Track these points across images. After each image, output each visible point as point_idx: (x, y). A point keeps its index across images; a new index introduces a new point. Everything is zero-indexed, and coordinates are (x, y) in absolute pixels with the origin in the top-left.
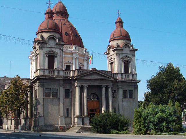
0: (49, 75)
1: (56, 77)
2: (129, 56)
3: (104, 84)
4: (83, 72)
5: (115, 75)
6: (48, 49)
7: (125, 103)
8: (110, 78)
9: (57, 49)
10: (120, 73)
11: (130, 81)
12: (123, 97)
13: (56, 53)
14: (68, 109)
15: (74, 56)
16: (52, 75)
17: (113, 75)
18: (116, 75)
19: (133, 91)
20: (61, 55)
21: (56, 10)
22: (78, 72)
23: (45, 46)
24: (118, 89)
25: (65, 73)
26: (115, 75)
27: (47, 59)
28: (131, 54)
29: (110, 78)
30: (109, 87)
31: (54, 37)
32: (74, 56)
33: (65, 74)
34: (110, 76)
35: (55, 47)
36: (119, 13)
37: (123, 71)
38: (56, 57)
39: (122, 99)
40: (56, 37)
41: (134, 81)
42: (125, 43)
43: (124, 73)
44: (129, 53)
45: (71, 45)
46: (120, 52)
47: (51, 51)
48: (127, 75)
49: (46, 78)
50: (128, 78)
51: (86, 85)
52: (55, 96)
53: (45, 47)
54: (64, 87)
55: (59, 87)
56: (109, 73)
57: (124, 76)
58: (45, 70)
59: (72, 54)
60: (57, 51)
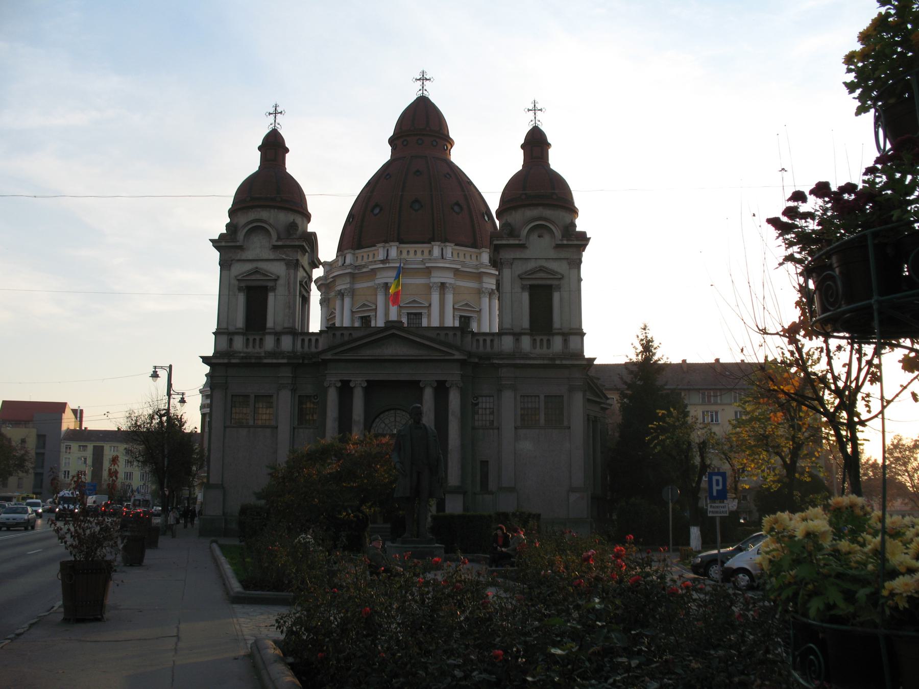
0: (245, 350)
1: (265, 358)
2: (554, 266)
5: (492, 341)
6: (248, 267)
7: (526, 446)
8: (454, 355)
10: (510, 334)
11: (546, 362)
13: (274, 277)
15: (437, 278)
16: (257, 349)
17: (485, 340)
18: (496, 342)
20: (289, 283)
22: (334, 335)
23: (238, 257)
25: (303, 340)
26: (492, 341)
27: (241, 298)
28: (560, 259)
29: (454, 355)
30: (447, 385)
33: (302, 347)
34: (450, 346)
35: (272, 257)
36: (535, 110)
37: (526, 324)
38: (274, 289)
39: (516, 428)
40: (270, 225)
41: (564, 362)
43: (529, 331)
44: (552, 254)
46: (518, 254)
48: (542, 340)
49: (233, 361)
51: (358, 380)
54: (294, 391)
56: (451, 333)
57: (526, 343)
60: (278, 269)
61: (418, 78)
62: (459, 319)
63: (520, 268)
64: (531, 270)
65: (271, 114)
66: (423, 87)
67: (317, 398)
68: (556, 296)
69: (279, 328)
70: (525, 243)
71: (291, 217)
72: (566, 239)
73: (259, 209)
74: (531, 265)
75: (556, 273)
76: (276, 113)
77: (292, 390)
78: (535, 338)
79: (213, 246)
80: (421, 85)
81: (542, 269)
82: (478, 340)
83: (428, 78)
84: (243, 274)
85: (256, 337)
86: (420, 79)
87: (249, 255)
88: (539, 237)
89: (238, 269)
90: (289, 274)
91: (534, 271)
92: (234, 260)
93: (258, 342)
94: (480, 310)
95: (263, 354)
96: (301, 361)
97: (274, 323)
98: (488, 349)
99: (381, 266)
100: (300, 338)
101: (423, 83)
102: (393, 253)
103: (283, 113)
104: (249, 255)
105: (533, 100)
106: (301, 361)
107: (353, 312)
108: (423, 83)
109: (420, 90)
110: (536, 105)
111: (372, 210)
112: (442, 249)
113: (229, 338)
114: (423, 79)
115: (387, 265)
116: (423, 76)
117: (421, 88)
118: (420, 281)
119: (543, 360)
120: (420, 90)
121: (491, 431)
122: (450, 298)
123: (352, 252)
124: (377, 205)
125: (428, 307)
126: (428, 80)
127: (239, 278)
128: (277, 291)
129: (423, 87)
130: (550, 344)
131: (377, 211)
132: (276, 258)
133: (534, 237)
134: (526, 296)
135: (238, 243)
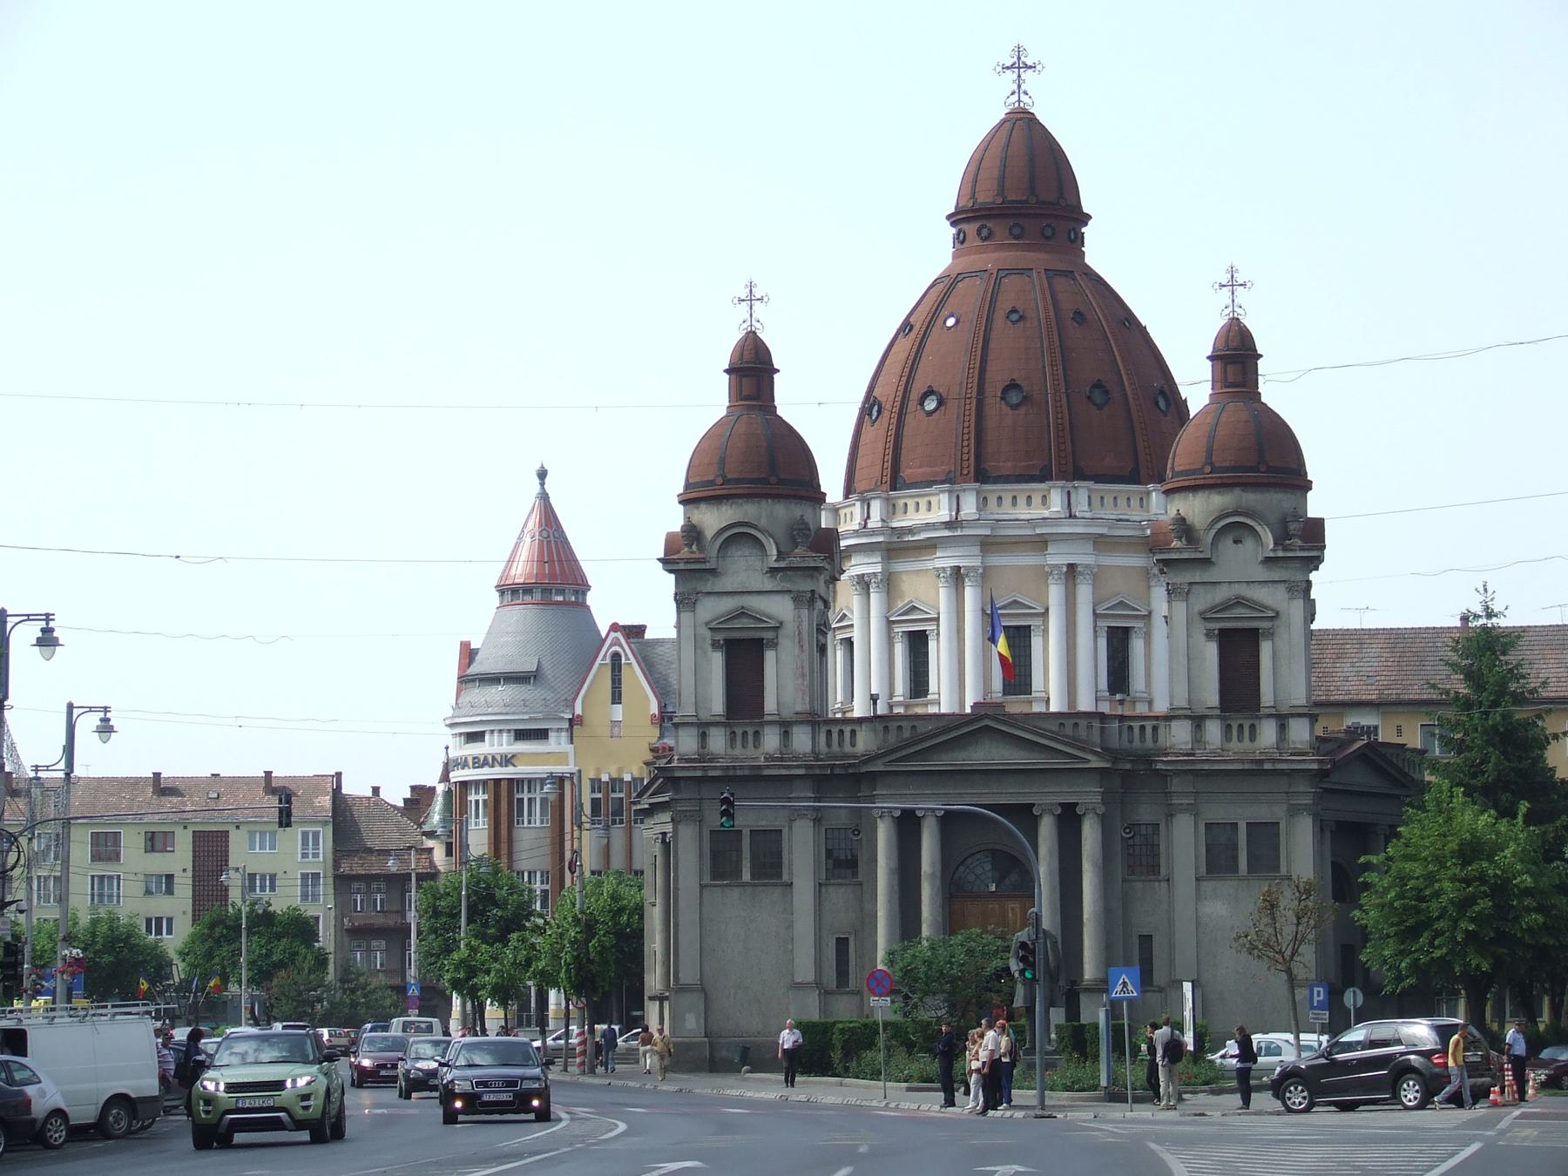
2: (1262, 595)
3: (1047, 797)
4: (914, 727)
5: (1155, 729)
6: (728, 604)
8: (1089, 761)
9: (778, 598)
10: (1186, 717)
11: (1247, 766)
12: (1203, 870)
13: (773, 624)
14: (842, 944)
16: (751, 751)
18: (1161, 731)
19: (1282, 826)
20: (800, 633)
21: (973, 196)
22: (886, 728)
23: (708, 588)
24: (1170, 816)
25: (829, 733)
26: (1155, 729)
27: (717, 661)
29: (1089, 761)
30: (1079, 811)
31: (753, 532)
32: (1058, 557)
33: (829, 744)
38: (774, 644)
39: (1197, 879)
42: (1235, 513)
43: (1217, 712)
44: (1262, 573)
45: (1043, 477)
47: (742, 613)
48: (1241, 726)
50: (1247, 742)
52: (770, 866)
53: (709, 593)
55: (791, 821)
57: (1213, 731)
58: (709, 724)
59: (1041, 543)
60: (780, 608)
61: (1009, 64)
62: (1105, 634)
63: (1204, 599)
64: (1222, 604)
65: (743, 300)
66: (1019, 86)
67: (858, 834)
68: (1266, 648)
69: (787, 714)
70: (1209, 556)
71: (799, 510)
72: (1280, 548)
73: (740, 501)
74: (1221, 594)
75: (1262, 607)
76: (751, 299)
77: (814, 820)
78: (1229, 722)
79: (666, 570)
80: (1014, 82)
81: (1239, 602)
82: (1131, 728)
83: (1029, 63)
84: (717, 619)
85: (747, 729)
86: (1012, 67)
87: (727, 583)
88: (1235, 542)
89: (711, 609)
90: (799, 617)
91: (1227, 606)
92: (701, 592)
93: (750, 738)
94: (1150, 613)
95: (762, 762)
96: (829, 772)
97: (778, 704)
98: (1149, 743)
99: (946, 533)
100: (824, 729)
101: (1019, 76)
102: (969, 507)
103: (765, 299)
104: (727, 583)
105: (1227, 266)
106: (829, 772)
107: (890, 623)
108: (1019, 76)
109: (1013, 93)
110: (1235, 275)
111: (922, 404)
112: (1069, 493)
113: (701, 731)
114: (1019, 66)
115: (959, 533)
116: (1019, 58)
117: (1015, 87)
118: (1028, 560)
119: (1243, 763)
120: (1013, 93)
121: (1157, 883)
122: (1084, 593)
123: (884, 495)
124: (930, 392)
125: (1043, 613)
126: (1031, 67)
127: (713, 625)
128: (779, 647)
129: (1019, 86)
130: (1255, 732)
131: (930, 405)
132: (775, 589)
133: (1227, 543)
134: (1211, 651)
135: (708, 564)
